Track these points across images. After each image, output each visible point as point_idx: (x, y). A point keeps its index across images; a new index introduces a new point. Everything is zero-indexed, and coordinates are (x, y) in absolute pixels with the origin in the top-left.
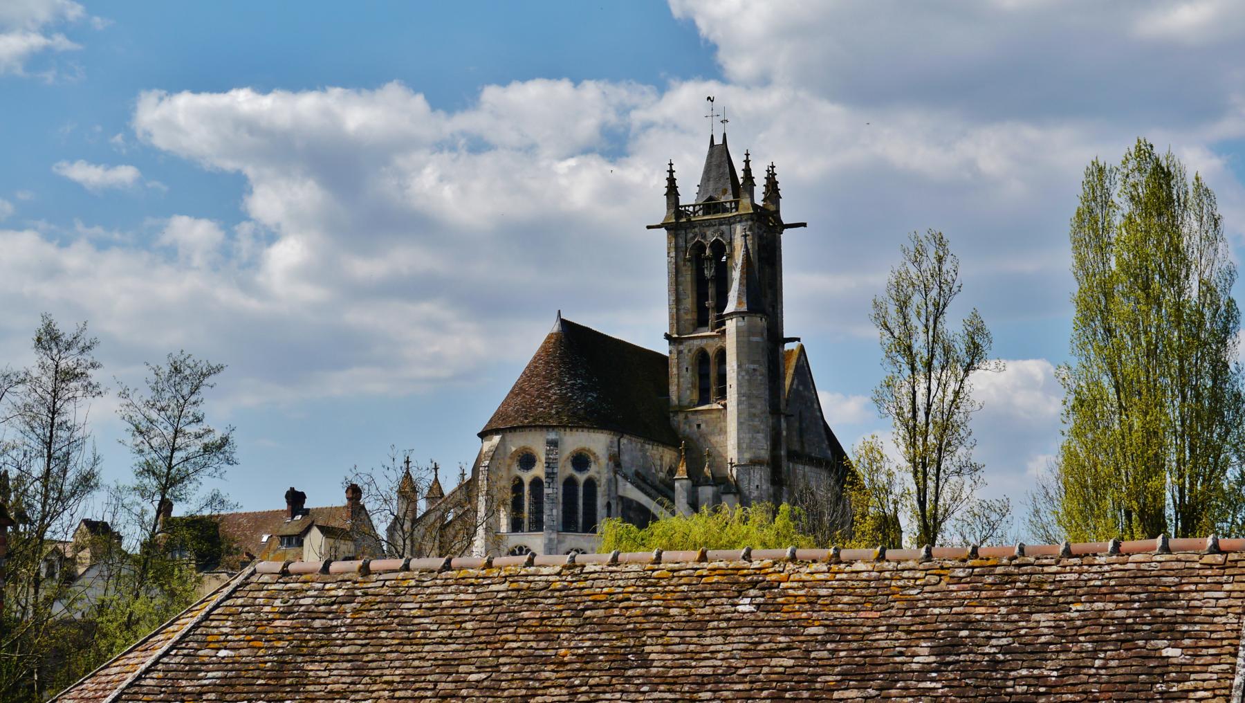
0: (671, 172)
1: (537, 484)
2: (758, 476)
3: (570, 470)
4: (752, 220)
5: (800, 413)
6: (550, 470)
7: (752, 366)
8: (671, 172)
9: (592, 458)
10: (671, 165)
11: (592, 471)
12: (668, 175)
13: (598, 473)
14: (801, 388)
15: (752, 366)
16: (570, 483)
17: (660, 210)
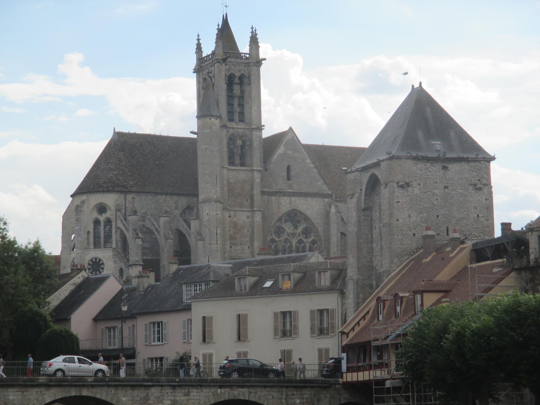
0: (198, 40)
1: (108, 222)
2: (208, 208)
3: (96, 215)
4: (219, 62)
5: (289, 168)
6: (77, 217)
7: (204, 147)
8: (198, 40)
9: (108, 208)
10: (198, 36)
11: (108, 214)
12: (197, 42)
13: (112, 215)
14: (289, 152)
15: (204, 147)
16: (97, 222)
17: (193, 62)
